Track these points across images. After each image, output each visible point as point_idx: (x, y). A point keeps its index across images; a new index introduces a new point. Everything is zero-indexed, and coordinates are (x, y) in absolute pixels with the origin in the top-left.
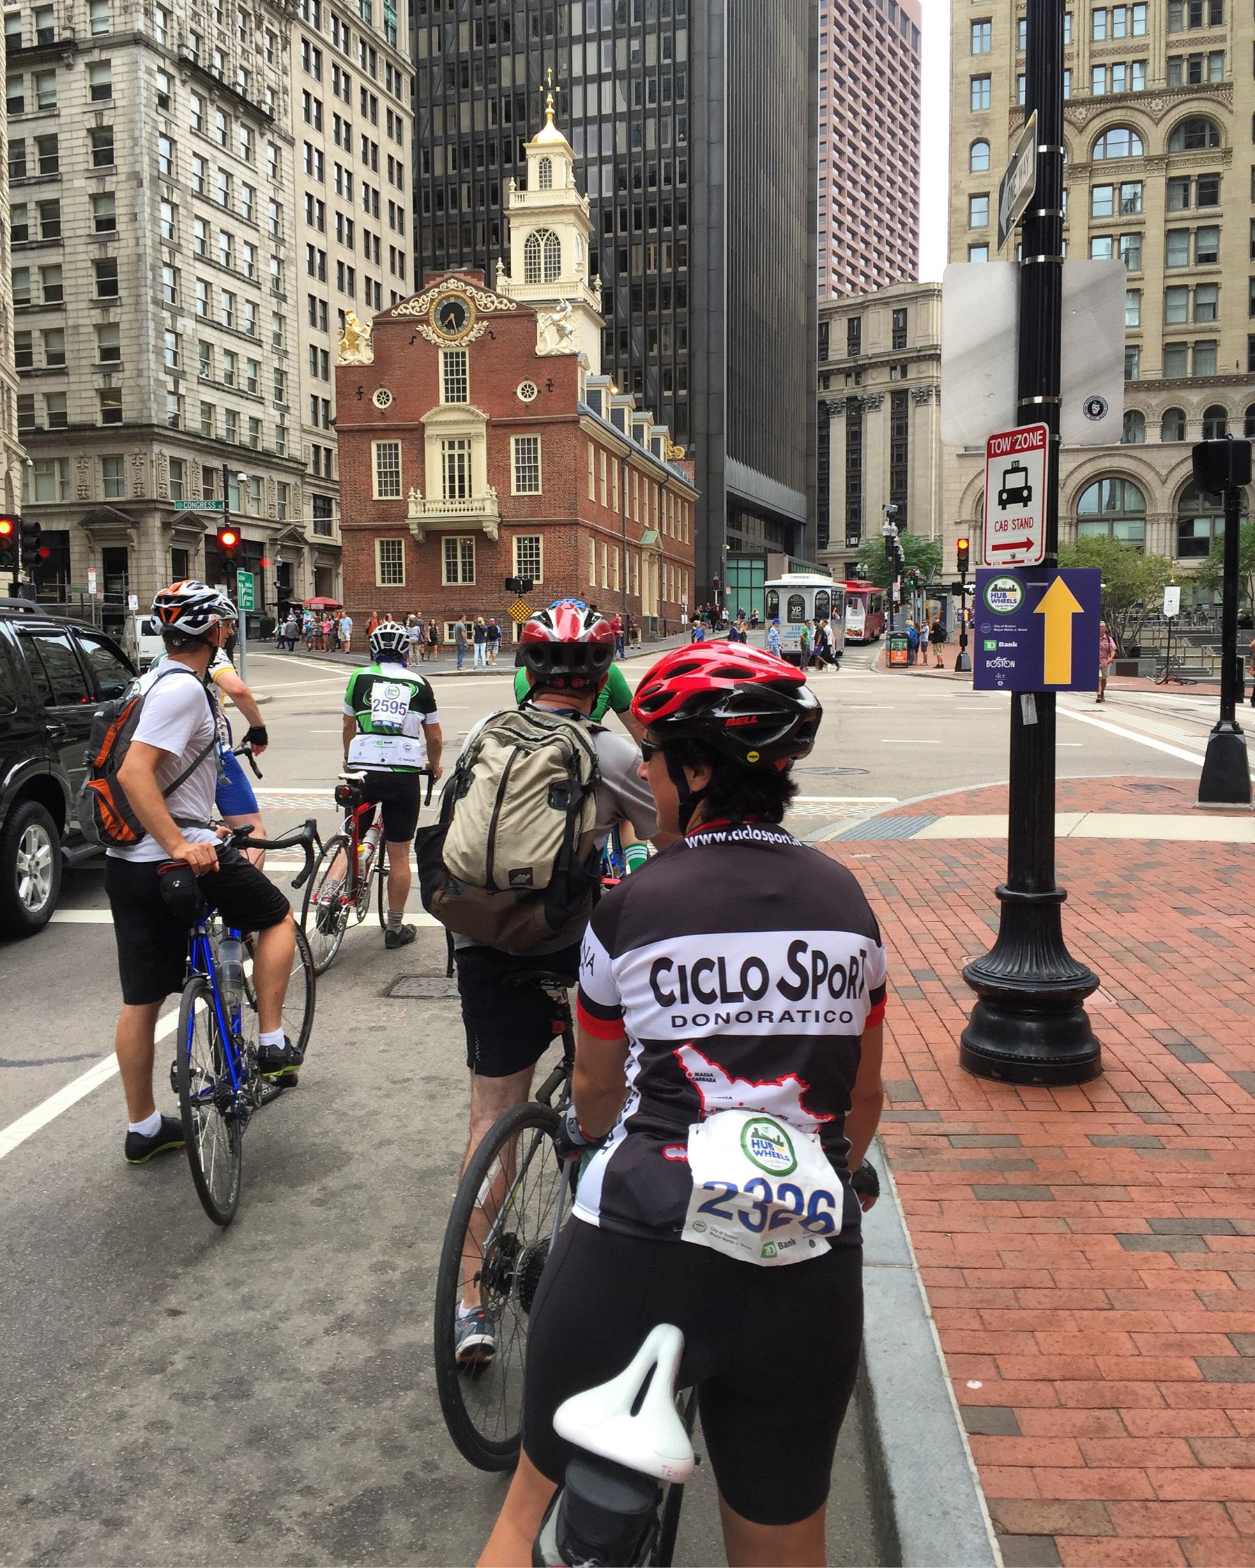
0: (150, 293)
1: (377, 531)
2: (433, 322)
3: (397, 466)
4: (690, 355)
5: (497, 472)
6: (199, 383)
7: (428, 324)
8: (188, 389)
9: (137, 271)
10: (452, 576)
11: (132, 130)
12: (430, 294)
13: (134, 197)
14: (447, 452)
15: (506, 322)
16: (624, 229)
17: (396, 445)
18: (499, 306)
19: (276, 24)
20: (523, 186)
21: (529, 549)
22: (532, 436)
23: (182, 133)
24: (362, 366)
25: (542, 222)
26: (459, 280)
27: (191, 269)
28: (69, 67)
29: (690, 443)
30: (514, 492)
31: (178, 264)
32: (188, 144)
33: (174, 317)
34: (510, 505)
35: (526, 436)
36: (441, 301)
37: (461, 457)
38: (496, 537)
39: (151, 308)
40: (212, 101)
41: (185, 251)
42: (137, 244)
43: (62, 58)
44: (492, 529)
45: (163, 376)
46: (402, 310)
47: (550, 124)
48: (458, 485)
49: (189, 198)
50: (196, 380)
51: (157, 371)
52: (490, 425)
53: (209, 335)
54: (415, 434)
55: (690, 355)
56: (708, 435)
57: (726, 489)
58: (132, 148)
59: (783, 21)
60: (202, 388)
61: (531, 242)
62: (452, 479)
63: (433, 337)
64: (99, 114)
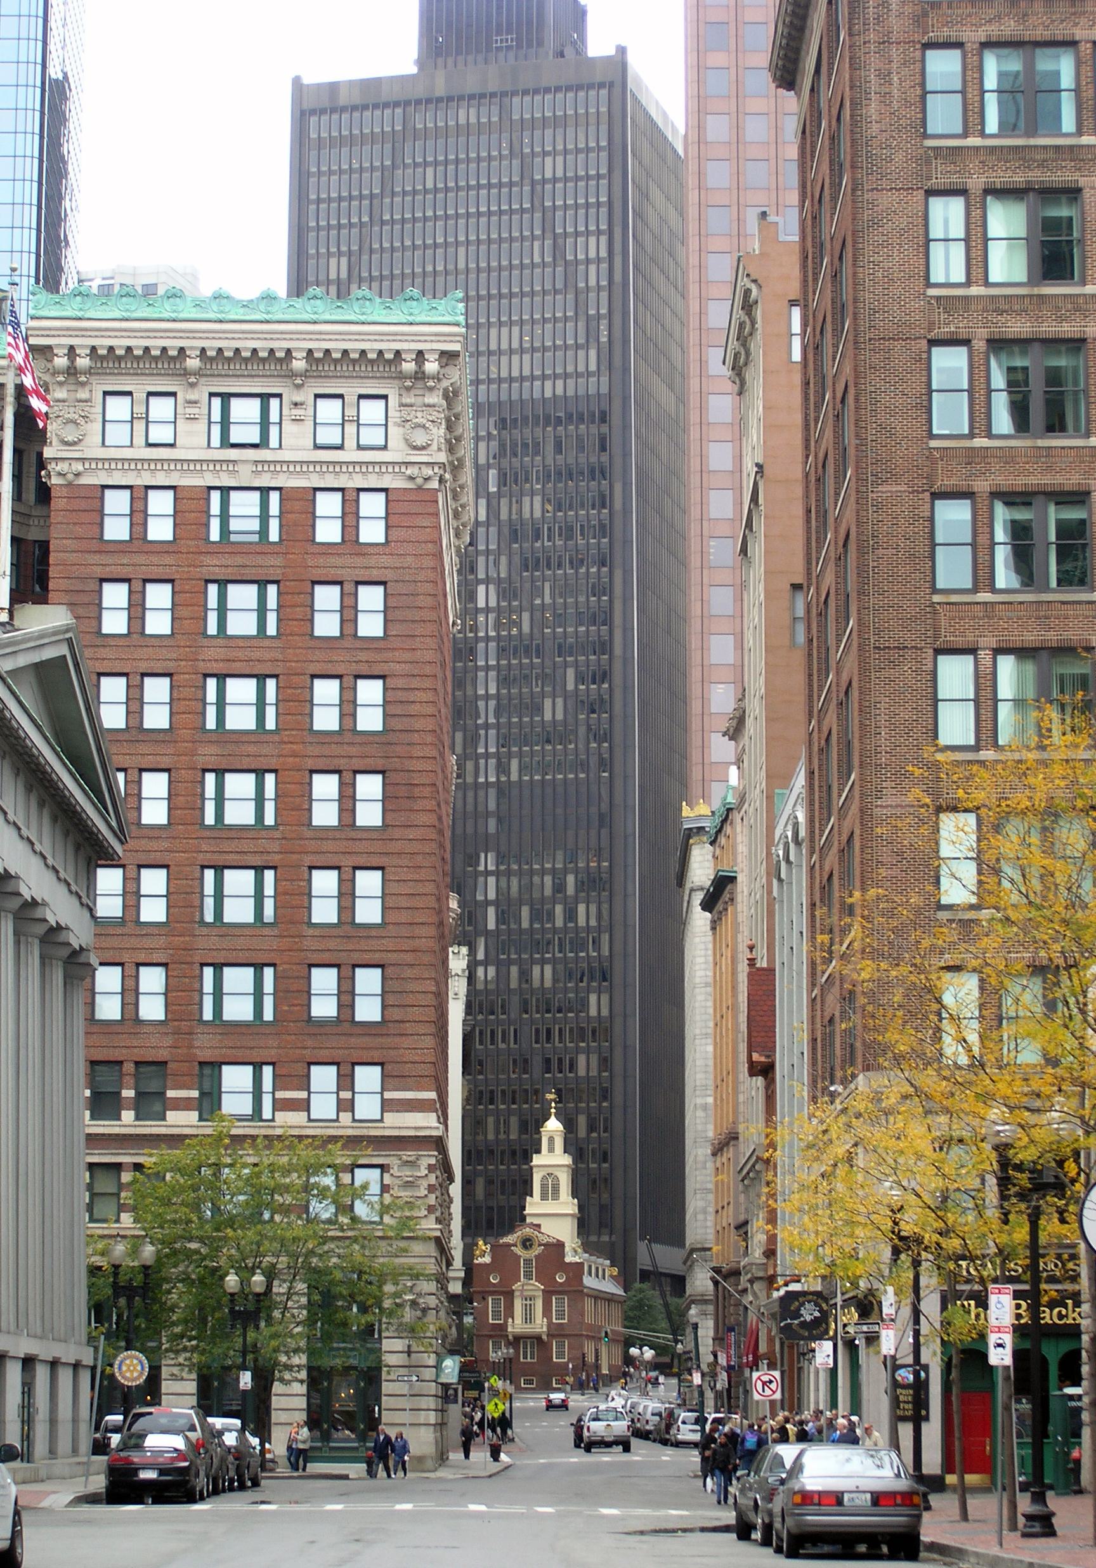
1: (491, 1337)
4: (611, 1169)
5: (547, 1312)
10: (525, 1357)
16: (560, 1072)
20: (538, 1151)
21: (560, 1345)
24: (486, 1265)
25: (550, 1170)
29: (611, 1234)
44: (545, 1337)
47: (553, 1118)
48: (528, 1318)
52: (543, 1290)
54: (509, 1295)
55: (611, 1169)
56: (625, 1230)
57: (639, 1267)
61: (544, 1178)
63: (519, 1253)
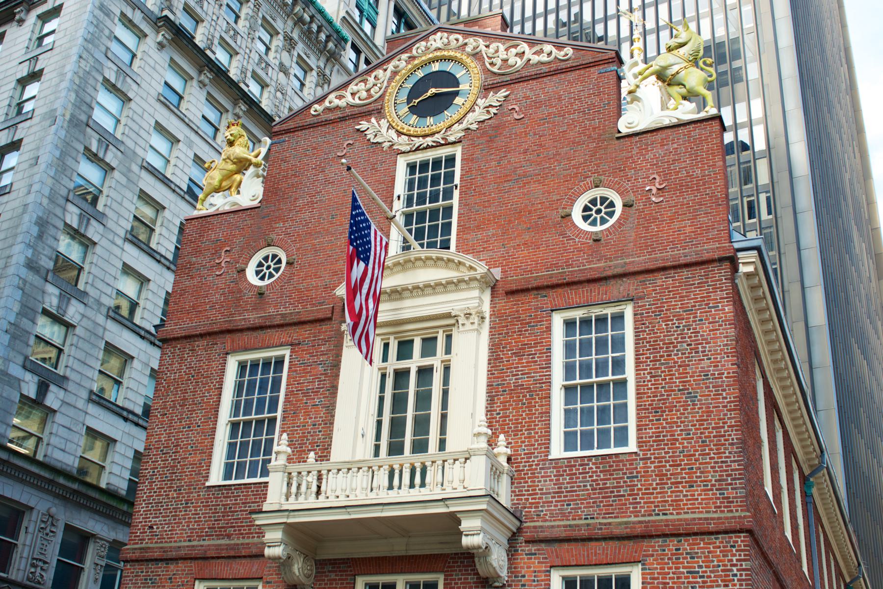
0: (29, 254)
2: (389, 108)
3: (273, 407)
6: (90, 400)
7: (379, 113)
8: (63, 402)
9: (17, 227)
11: (64, 66)
12: (391, 67)
13: (42, 139)
14: (393, 364)
15: (551, 85)
17: (280, 362)
18: (535, 59)
19: (312, 57)
22: (609, 311)
23: (141, 92)
26: (451, 31)
27: (118, 252)
28: (21, 22)
30: (557, 450)
31: (93, 231)
32: (146, 107)
33: (65, 297)
34: (547, 485)
35: (596, 312)
36: (412, 73)
37: (425, 373)
38: (504, 574)
39: (24, 272)
40: (202, 84)
41: (110, 224)
42: (29, 193)
43: (14, 14)
45: (16, 370)
46: (333, 100)
49: (135, 168)
50: (85, 395)
51: (7, 360)
53: (126, 340)
58: (58, 85)
59: (854, 228)
60: (92, 409)
62: (397, 427)
64: (36, 58)
